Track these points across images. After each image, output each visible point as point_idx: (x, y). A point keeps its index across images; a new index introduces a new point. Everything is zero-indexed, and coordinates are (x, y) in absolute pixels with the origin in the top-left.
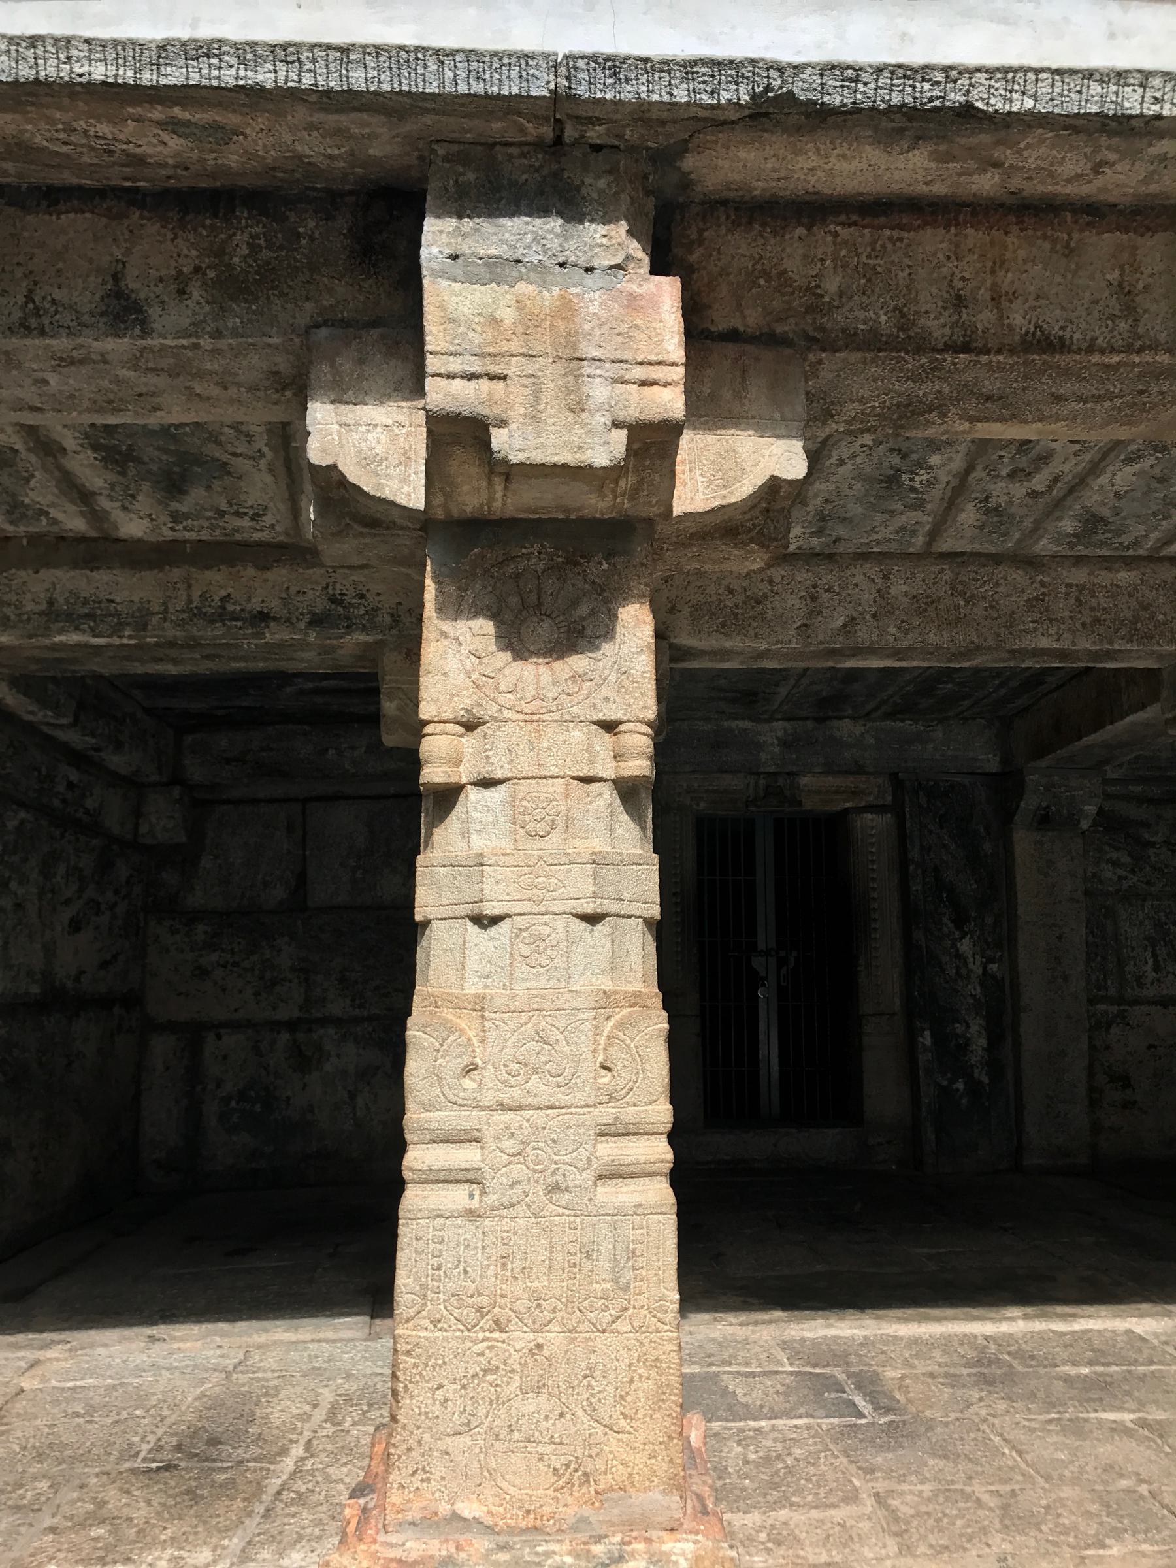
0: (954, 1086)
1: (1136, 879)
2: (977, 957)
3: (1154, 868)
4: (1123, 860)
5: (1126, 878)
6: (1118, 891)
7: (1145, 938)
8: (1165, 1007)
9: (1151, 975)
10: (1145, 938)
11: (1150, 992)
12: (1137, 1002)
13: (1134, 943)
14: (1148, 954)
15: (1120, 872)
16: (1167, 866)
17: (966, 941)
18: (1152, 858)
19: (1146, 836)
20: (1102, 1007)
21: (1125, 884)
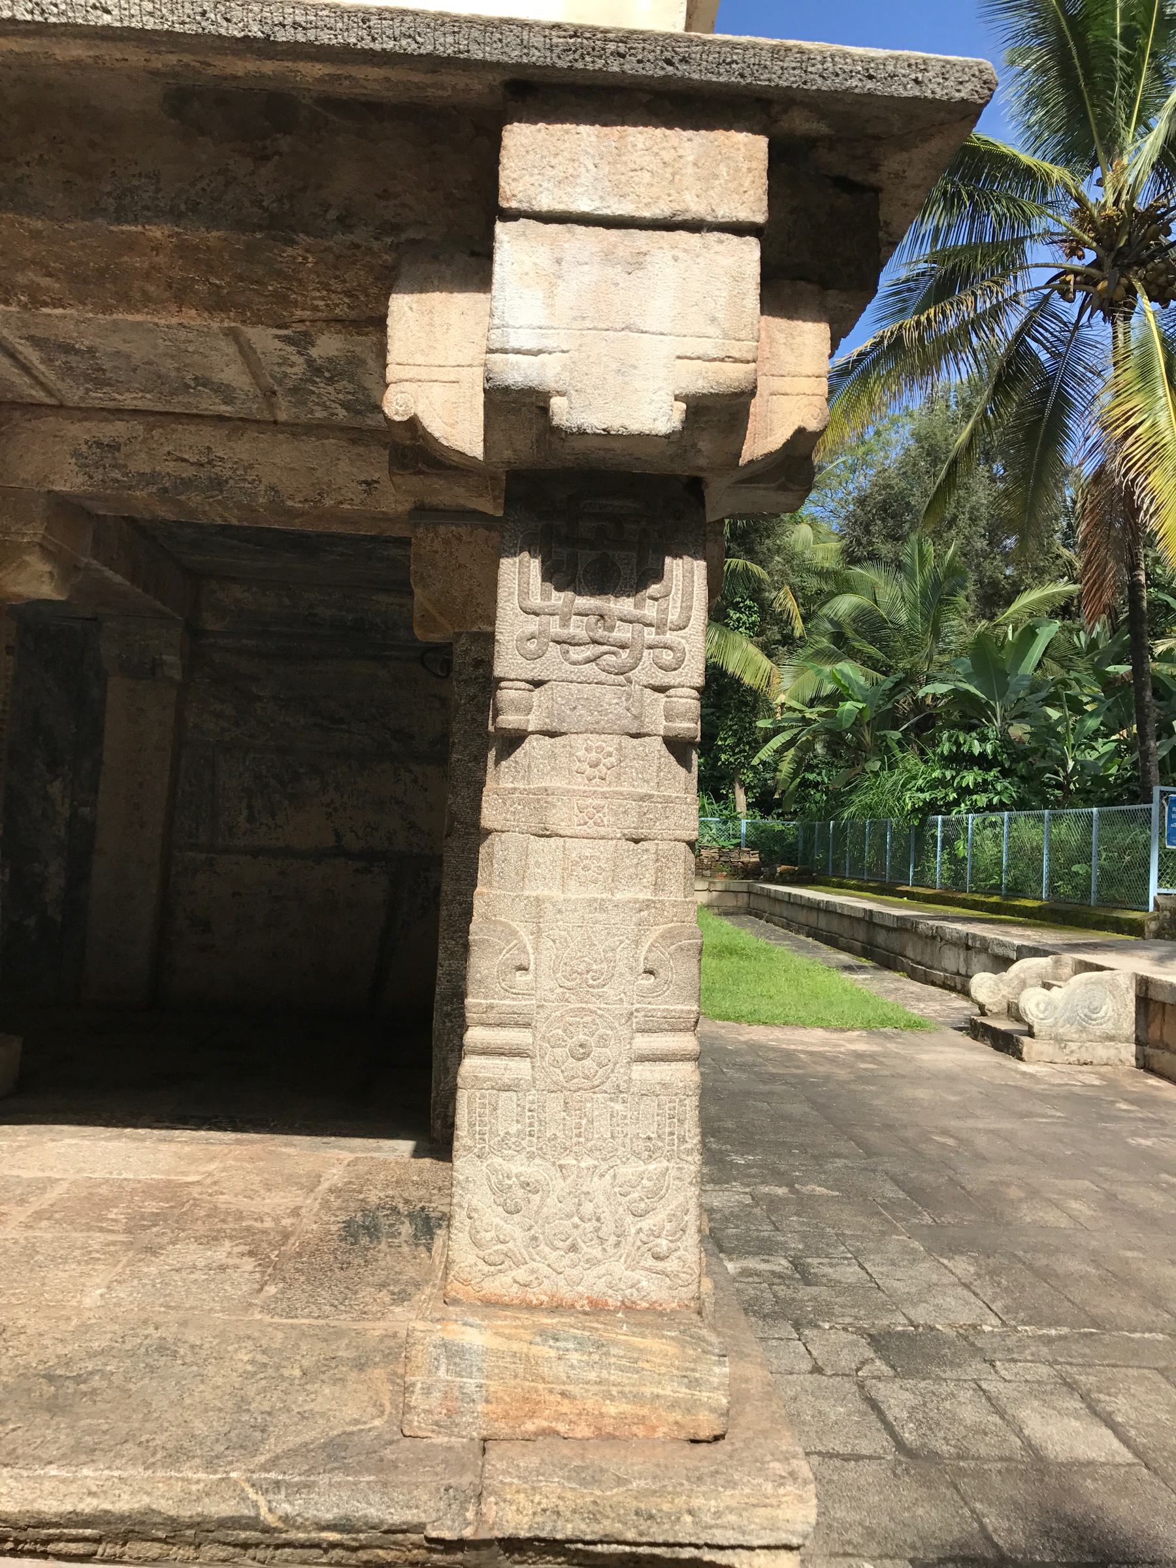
0: (25, 923)
2: (66, 800)
17: (57, 784)
20: (191, 854)
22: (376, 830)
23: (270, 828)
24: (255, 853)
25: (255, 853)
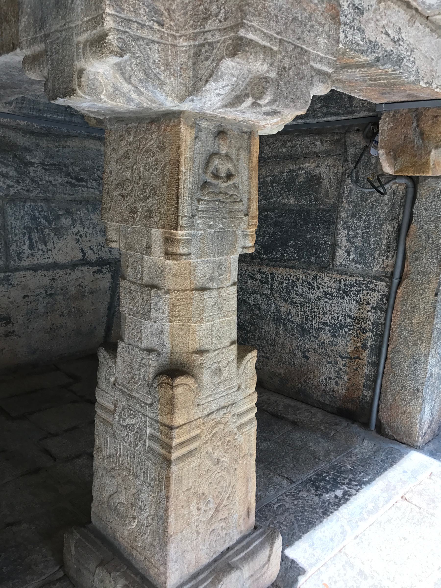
1: (19, 188)
3: (33, 181)
4: (11, 174)
5: (13, 186)
6: (6, 195)
7: (24, 228)
8: (36, 271)
9: (28, 252)
10: (24, 228)
11: (26, 263)
12: (17, 269)
13: (17, 231)
14: (26, 238)
15: (9, 182)
16: (41, 180)
18: (32, 174)
19: (28, 158)
21: (12, 191)
22: (104, 247)
23: (44, 252)
24: (35, 268)
25: (35, 268)
